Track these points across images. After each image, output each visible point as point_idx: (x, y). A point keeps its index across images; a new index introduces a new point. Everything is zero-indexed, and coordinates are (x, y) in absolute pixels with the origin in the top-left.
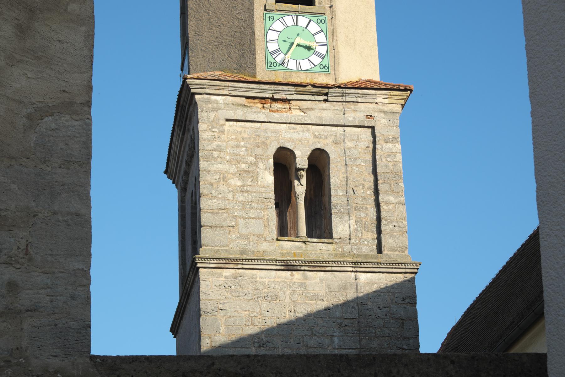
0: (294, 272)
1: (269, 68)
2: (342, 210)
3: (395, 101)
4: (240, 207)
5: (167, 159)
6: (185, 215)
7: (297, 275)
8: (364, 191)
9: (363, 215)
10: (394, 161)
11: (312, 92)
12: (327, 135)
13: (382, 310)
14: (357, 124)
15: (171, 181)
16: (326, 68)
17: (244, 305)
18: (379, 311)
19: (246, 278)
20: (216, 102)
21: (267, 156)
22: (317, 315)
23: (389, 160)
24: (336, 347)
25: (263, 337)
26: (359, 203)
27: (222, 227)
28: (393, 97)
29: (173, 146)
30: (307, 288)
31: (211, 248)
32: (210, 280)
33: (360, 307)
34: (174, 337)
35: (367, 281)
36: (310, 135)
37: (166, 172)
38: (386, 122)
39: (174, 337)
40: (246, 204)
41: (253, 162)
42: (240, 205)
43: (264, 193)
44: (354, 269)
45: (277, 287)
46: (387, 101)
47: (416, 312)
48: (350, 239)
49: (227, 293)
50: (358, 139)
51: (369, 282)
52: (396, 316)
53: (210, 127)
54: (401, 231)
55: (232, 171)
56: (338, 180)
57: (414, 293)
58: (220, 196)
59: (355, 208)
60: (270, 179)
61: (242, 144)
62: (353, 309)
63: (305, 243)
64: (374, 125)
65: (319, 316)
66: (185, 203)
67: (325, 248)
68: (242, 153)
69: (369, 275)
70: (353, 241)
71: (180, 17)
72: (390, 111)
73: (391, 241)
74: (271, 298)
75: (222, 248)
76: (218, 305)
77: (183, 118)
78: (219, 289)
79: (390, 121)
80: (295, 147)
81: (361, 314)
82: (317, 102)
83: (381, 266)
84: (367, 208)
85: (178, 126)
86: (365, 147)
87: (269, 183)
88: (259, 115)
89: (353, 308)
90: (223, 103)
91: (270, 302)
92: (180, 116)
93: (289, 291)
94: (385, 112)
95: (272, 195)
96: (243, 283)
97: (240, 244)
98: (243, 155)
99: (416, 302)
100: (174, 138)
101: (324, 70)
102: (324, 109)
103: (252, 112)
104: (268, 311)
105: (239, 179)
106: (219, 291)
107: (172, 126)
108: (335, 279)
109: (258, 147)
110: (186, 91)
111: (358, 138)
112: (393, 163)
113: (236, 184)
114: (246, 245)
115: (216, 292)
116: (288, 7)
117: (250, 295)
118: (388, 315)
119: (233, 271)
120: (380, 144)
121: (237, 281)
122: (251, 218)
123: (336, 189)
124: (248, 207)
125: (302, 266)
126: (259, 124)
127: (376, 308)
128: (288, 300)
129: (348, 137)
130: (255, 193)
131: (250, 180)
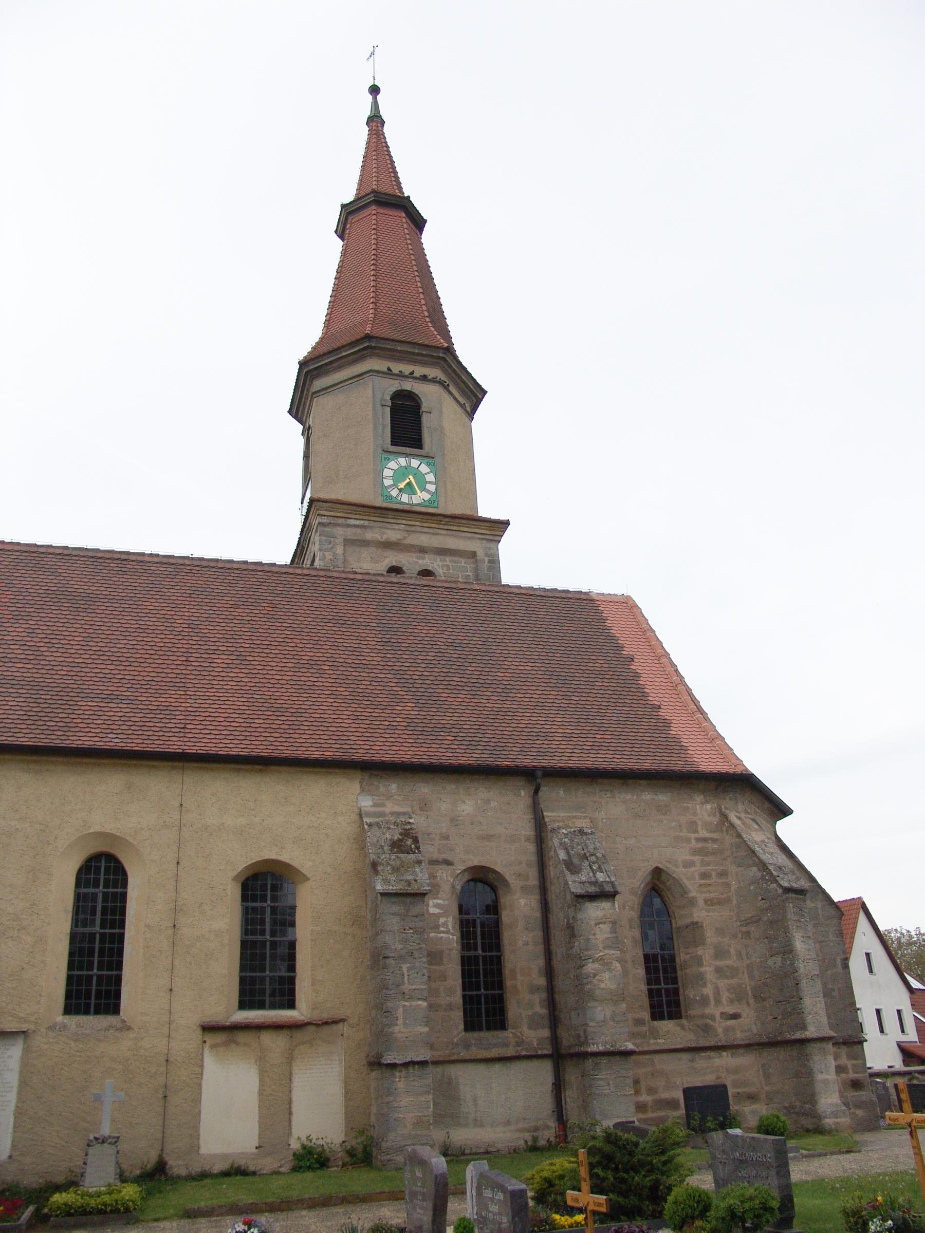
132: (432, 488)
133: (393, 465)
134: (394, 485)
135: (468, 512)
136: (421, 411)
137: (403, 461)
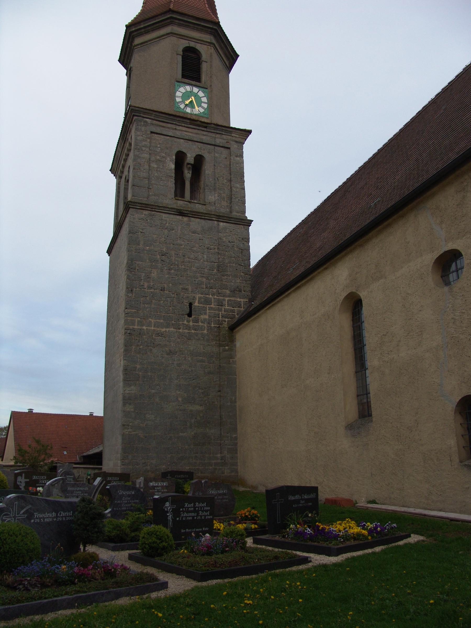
0: (184, 217)
2: (211, 188)
3: (242, 137)
6: (120, 191)
7: (185, 219)
9: (222, 192)
11: (199, 125)
14: (221, 145)
15: (113, 175)
17: (154, 231)
18: (229, 243)
19: (157, 217)
24: (205, 260)
25: (164, 250)
27: (144, 188)
29: (117, 152)
30: (191, 226)
32: (136, 215)
34: (109, 256)
35: (223, 227)
37: (110, 170)
39: (109, 256)
44: (217, 219)
45: (173, 223)
46: (238, 136)
47: (249, 247)
48: (215, 204)
59: (218, 188)
60: (173, 166)
61: (159, 146)
64: (230, 147)
67: (201, 207)
68: (158, 151)
69: (225, 224)
70: (216, 205)
71: (126, 90)
73: (237, 207)
75: (144, 199)
81: (219, 244)
82: (201, 131)
84: (224, 189)
85: (122, 138)
86: (225, 158)
90: (149, 123)
94: (236, 142)
95: (173, 175)
100: (119, 146)
102: (204, 135)
109: (167, 149)
116: (188, 82)
117: (158, 226)
119: (149, 212)
122: (161, 185)
124: (160, 179)
125: (188, 214)
126: (169, 137)
128: (179, 231)
131: (161, 165)
132: (205, 106)
133: (182, 90)
134: (182, 101)
135: (227, 125)
136: (201, 61)
137: (188, 88)
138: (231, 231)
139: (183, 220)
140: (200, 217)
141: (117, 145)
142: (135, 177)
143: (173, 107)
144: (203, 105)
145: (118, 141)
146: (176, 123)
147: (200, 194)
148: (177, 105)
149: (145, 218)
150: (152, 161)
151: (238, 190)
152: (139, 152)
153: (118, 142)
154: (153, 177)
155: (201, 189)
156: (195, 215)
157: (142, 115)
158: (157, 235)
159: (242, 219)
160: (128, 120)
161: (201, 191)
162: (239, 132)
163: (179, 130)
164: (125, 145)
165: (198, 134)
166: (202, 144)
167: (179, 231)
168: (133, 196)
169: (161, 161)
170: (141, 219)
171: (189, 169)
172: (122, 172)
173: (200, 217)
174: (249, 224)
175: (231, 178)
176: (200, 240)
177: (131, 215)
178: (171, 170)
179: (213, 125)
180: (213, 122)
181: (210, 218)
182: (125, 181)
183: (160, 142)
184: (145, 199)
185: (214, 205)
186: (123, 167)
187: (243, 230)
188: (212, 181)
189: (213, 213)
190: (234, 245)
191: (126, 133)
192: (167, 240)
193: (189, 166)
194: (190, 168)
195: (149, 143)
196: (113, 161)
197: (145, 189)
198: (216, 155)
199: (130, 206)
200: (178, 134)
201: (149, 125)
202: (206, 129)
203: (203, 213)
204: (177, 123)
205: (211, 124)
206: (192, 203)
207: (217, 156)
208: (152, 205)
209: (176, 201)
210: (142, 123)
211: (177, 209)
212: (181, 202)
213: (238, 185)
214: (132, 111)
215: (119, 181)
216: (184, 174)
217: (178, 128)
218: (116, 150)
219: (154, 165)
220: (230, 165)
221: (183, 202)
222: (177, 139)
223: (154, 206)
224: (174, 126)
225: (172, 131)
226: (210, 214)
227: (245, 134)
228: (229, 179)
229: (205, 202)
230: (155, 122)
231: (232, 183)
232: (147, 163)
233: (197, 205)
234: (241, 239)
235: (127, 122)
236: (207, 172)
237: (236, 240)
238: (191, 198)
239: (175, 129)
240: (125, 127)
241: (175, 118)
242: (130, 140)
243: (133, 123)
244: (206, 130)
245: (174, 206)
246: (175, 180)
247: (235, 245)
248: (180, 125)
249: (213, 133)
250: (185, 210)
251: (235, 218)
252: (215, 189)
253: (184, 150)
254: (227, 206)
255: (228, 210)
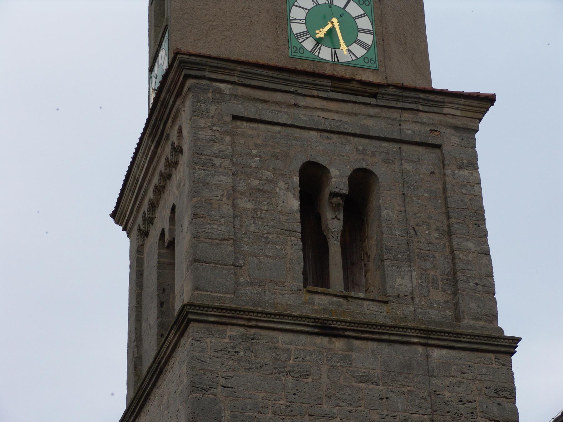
0: (334, 339)
1: (293, 54)
2: (399, 256)
3: (469, 114)
4: (251, 240)
5: (119, 192)
6: (143, 271)
7: (339, 344)
8: (429, 232)
9: (428, 265)
10: (471, 194)
12: (376, 151)
13: (465, 405)
14: (417, 140)
16: (372, 62)
17: (258, 382)
18: (461, 406)
19: (262, 341)
20: (219, 91)
21: (291, 172)
22: (369, 405)
23: (464, 193)
26: (424, 249)
28: (467, 108)
29: (135, 168)
30: (354, 364)
31: (208, 293)
32: (208, 341)
33: (433, 398)
36: (350, 149)
37: (113, 215)
38: (458, 140)
40: (260, 236)
41: (269, 178)
42: (251, 236)
43: (285, 222)
44: (422, 341)
45: (308, 358)
46: (458, 113)
48: (412, 299)
49: (233, 362)
50: (419, 161)
51: (444, 361)
52: (486, 415)
53: (209, 124)
54: (486, 292)
55: (240, 188)
56: (392, 214)
57: (511, 382)
58: (223, 220)
60: (295, 204)
61: (255, 152)
62: (423, 401)
63: (347, 300)
65: (372, 407)
66: (143, 255)
67: (375, 308)
68: (254, 165)
69: (444, 352)
70: (417, 301)
72: (464, 127)
73: (473, 305)
74: (299, 374)
76: (218, 379)
77: (161, 120)
78: (221, 355)
79: (462, 139)
80: (331, 163)
81: (435, 408)
82: (361, 106)
83: (463, 340)
84: (434, 257)
85: (151, 133)
86: (428, 172)
87: (293, 210)
88: (279, 114)
89: (422, 398)
90: (228, 93)
91: (297, 380)
92: (157, 118)
93: (326, 367)
94: (456, 128)
95: (298, 227)
96: (257, 348)
97: (251, 293)
98: (256, 168)
99: (515, 397)
101: (369, 64)
102: (371, 116)
103: (269, 109)
104: (294, 394)
105: (249, 201)
106: (220, 357)
107: (140, 136)
108: (394, 353)
110: (176, 73)
111: (419, 159)
112: (470, 197)
113: (245, 206)
114: (259, 294)
115: (216, 359)
118: (475, 413)
119: (242, 330)
120: (450, 169)
121: (249, 344)
122: (267, 256)
123: (390, 226)
124: (263, 240)
126: (278, 128)
127: (457, 401)
128: (324, 379)
129: (404, 157)
130: (273, 221)
132: (368, 39)
135: (420, 85)
138: (465, 370)
139: (332, 346)
140: (377, 337)
141: (134, 150)
142: (199, 237)
143: (286, 47)
144: (362, 37)
145: (138, 141)
146: (297, 89)
147: (369, 274)
148: (294, 43)
149: (233, 348)
150: (241, 193)
151: (471, 256)
152: (204, 170)
153: (139, 145)
154: (245, 234)
155: (371, 259)
156: (363, 332)
157: (208, 74)
158: (266, 392)
159: (492, 337)
160: (170, 86)
161: (372, 265)
162: (462, 102)
163: (306, 107)
164: (159, 151)
165: (356, 114)
166: (367, 141)
167: (324, 379)
168: (197, 288)
169: (265, 192)
170: (221, 350)
171: (335, 208)
172: (149, 221)
173: (377, 337)
174: (512, 350)
175: (449, 226)
176: (382, 399)
177: (193, 342)
178: (291, 213)
179: (392, 90)
180: (390, 83)
181: (405, 339)
182: (159, 245)
183: (259, 142)
184: (229, 296)
185: (411, 301)
186: (153, 206)
187: (494, 366)
188: (401, 238)
189: (410, 325)
190: (475, 409)
191: (163, 122)
192: (294, 405)
193: (335, 200)
194: (339, 205)
195: (230, 147)
196: (123, 190)
197: (226, 269)
198: (407, 166)
199: (190, 316)
200: (303, 117)
201: (228, 98)
202: (374, 99)
203: (386, 326)
204: (300, 91)
205: (388, 85)
206: (352, 300)
207: (409, 168)
208: (249, 312)
209: (308, 296)
210: (210, 95)
211: (315, 319)
212: (323, 297)
213: (471, 245)
214: (182, 64)
215: (141, 243)
216: (323, 220)
217: (302, 101)
218: (132, 163)
219: (246, 204)
220: (445, 190)
221: (329, 298)
222: (302, 131)
223: (253, 312)
224: (291, 99)
225: (286, 110)
226: (403, 328)
227: (477, 105)
228: (445, 228)
229: (386, 295)
230: (241, 90)
231: (455, 240)
232: (228, 199)
233: (366, 303)
234: (491, 393)
235: (167, 94)
236: (384, 213)
237: (480, 395)
238: (347, 288)
239: (295, 105)
240: (162, 105)
241: (294, 77)
242: (174, 137)
243: (186, 95)
244: (375, 103)
245: (307, 311)
246: (303, 239)
247: (477, 410)
248: (307, 93)
249: (393, 110)
250: (337, 321)
251: (470, 335)
252: (409, 259)
253: (322, 160)
254: (446, 302)
255: (448, 313)
